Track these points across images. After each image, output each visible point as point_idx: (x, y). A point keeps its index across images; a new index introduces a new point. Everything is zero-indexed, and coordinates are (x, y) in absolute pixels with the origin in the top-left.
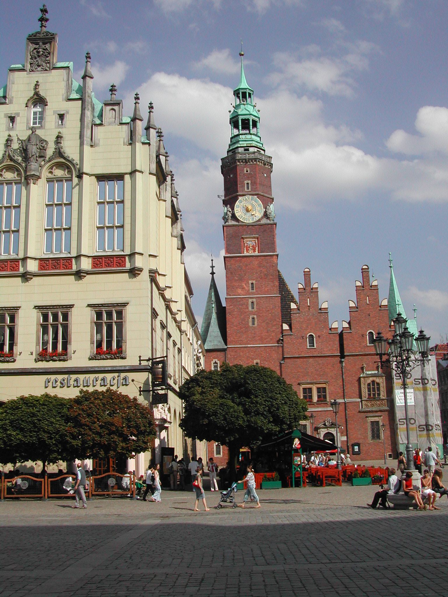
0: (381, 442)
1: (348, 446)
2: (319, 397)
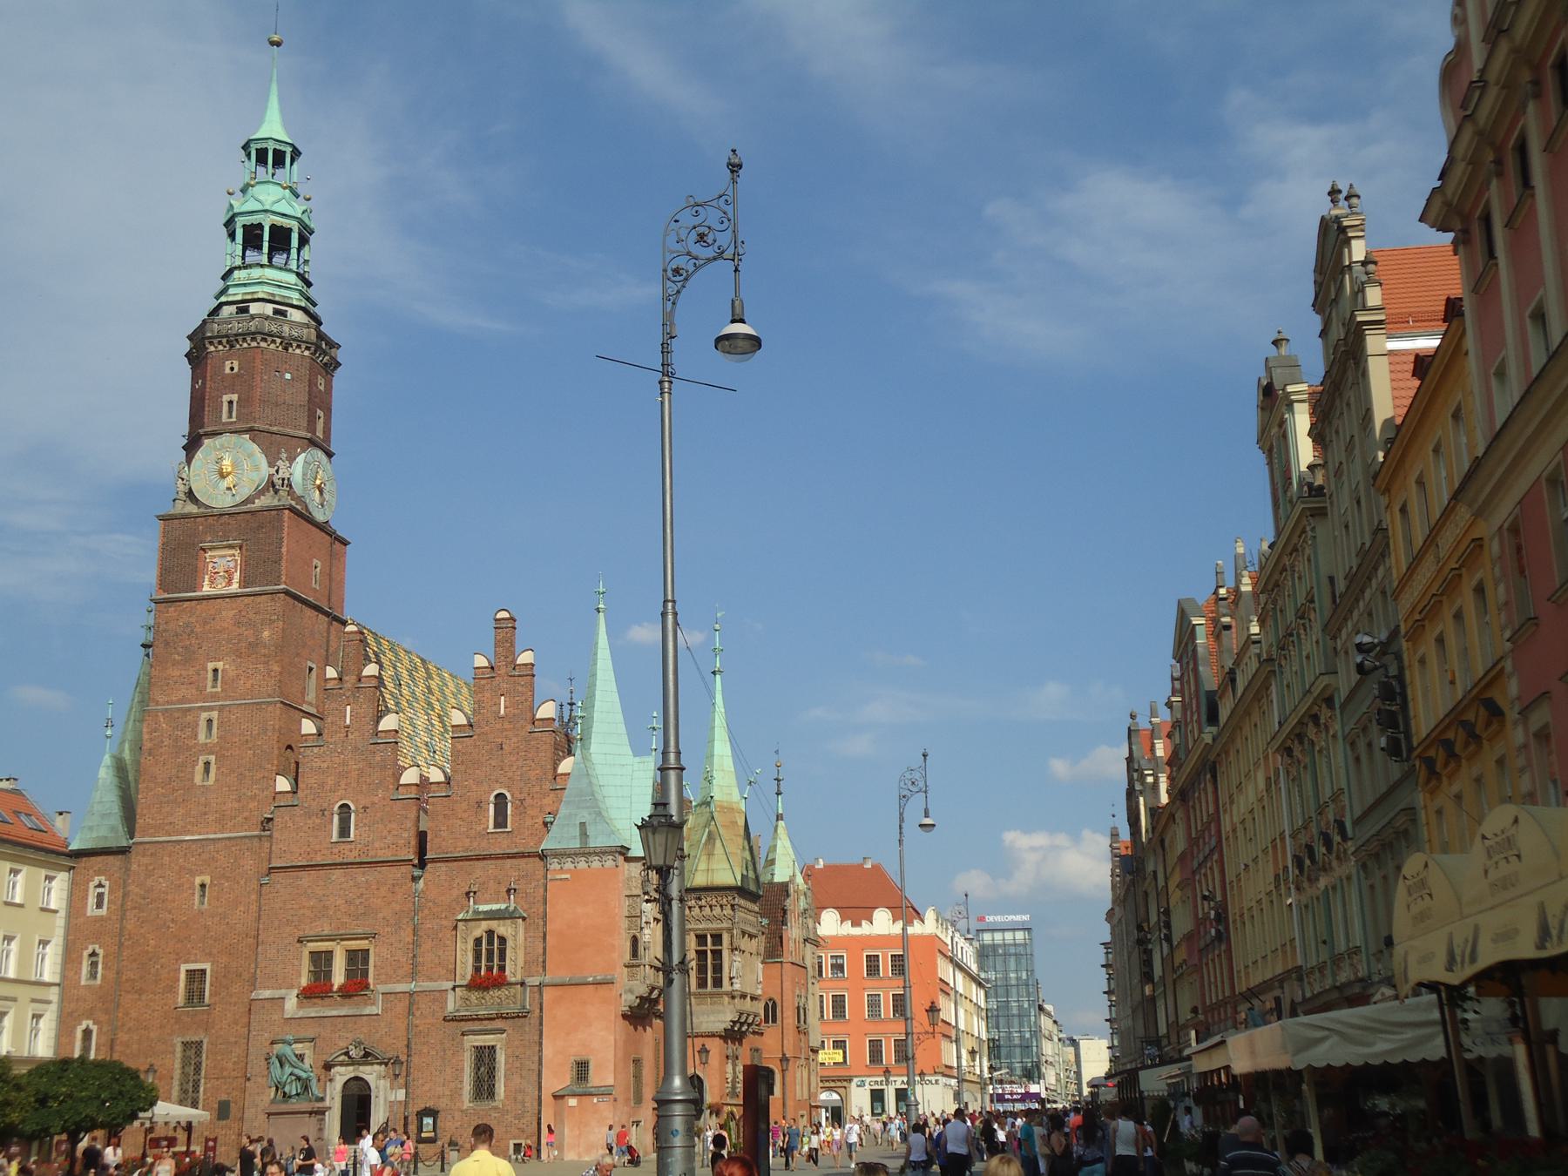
0: (496, 1108)
1: (406, 1118)
2: (349, 973)
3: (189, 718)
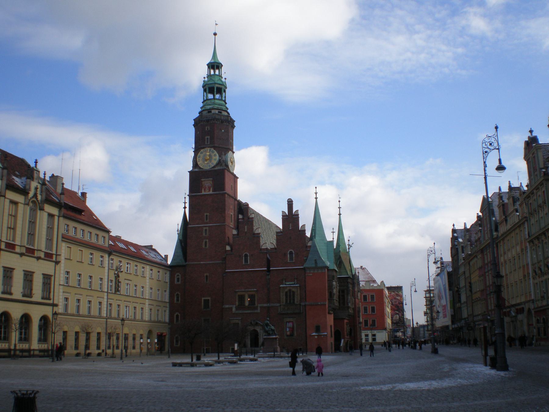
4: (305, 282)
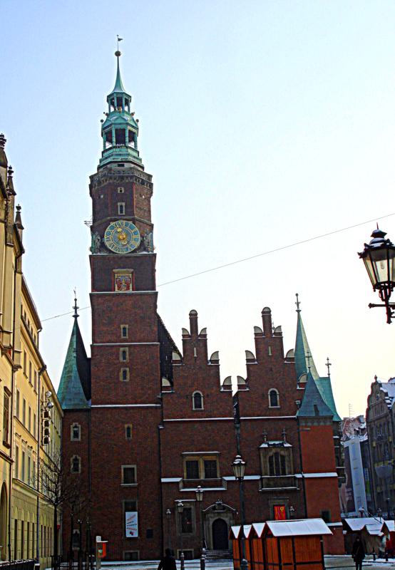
3: (114, 350)
4: (299, 440)
